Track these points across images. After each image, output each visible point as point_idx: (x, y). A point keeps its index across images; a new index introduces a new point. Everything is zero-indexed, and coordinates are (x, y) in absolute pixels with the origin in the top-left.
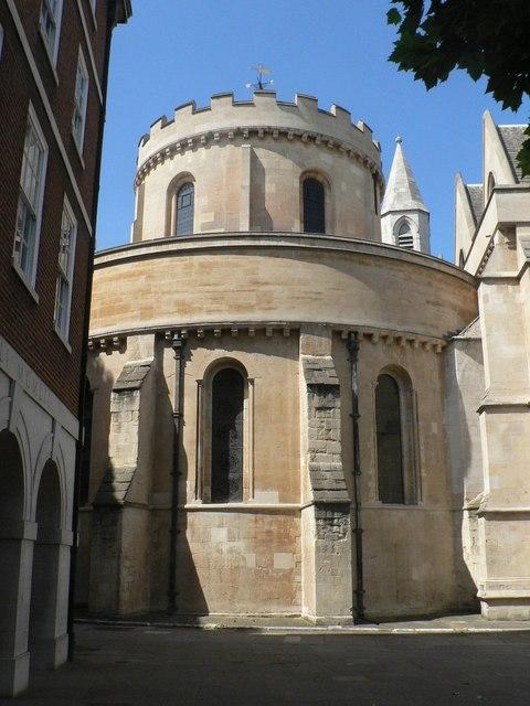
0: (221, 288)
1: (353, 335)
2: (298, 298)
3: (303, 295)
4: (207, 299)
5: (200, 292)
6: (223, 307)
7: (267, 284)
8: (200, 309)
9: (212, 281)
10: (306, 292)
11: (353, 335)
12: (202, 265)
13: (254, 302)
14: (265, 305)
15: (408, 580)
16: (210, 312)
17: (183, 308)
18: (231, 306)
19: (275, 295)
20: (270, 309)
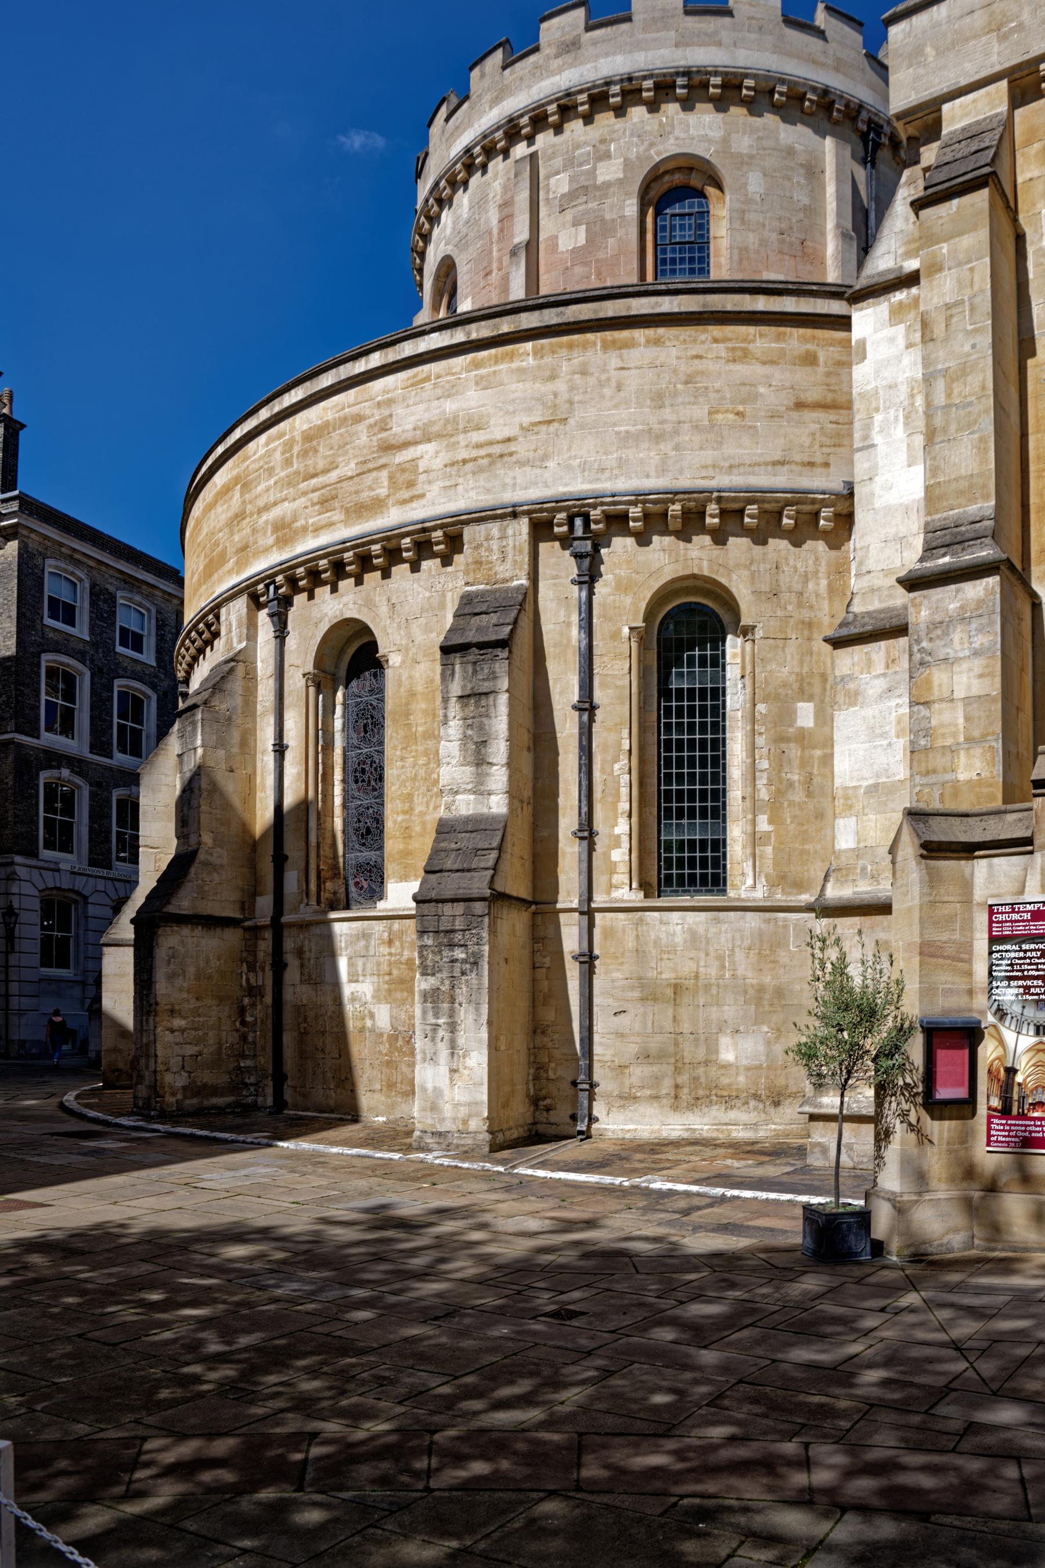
0: (333, 476)
1: (578, 522)
2: (465, 462)
3: (475, 453)
4: (313, 505)
5: (305, 493)
6: (337, 516)
7: (406, 445)
8: (305, 529)
9: (321, 465)
10: (478, 446)
11: (578, 522)
12: (309, 437)
13: (383, 492)
14: (406, 494)
15: (707, 1063)
16: (317, 530)
17: (285, 531)
18: (347, 511)
19: (422, 465)
20: (412, 499)
